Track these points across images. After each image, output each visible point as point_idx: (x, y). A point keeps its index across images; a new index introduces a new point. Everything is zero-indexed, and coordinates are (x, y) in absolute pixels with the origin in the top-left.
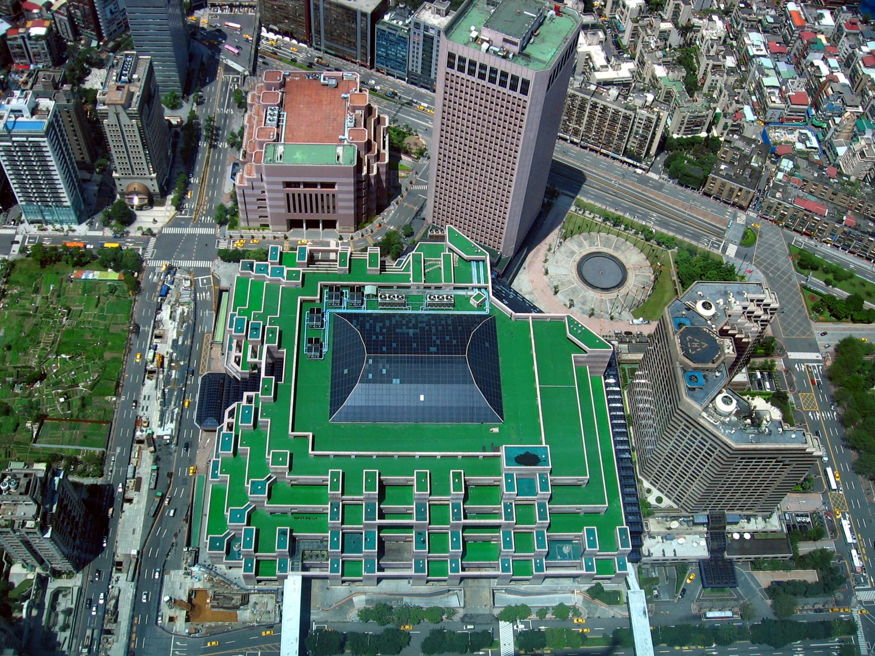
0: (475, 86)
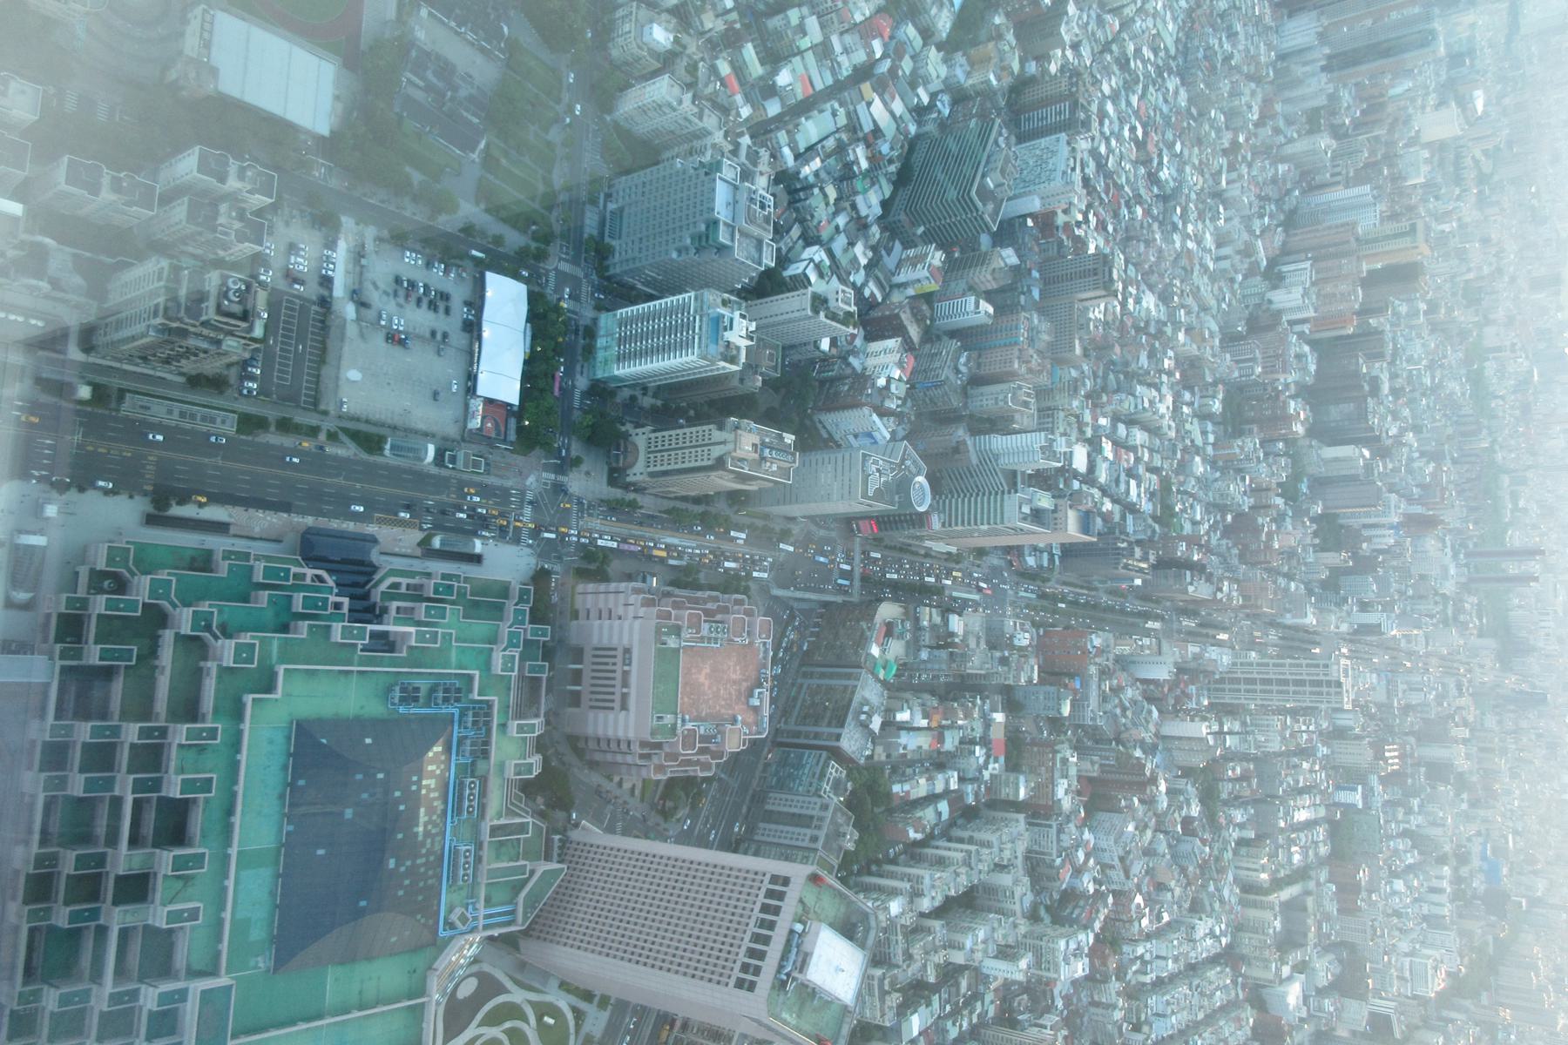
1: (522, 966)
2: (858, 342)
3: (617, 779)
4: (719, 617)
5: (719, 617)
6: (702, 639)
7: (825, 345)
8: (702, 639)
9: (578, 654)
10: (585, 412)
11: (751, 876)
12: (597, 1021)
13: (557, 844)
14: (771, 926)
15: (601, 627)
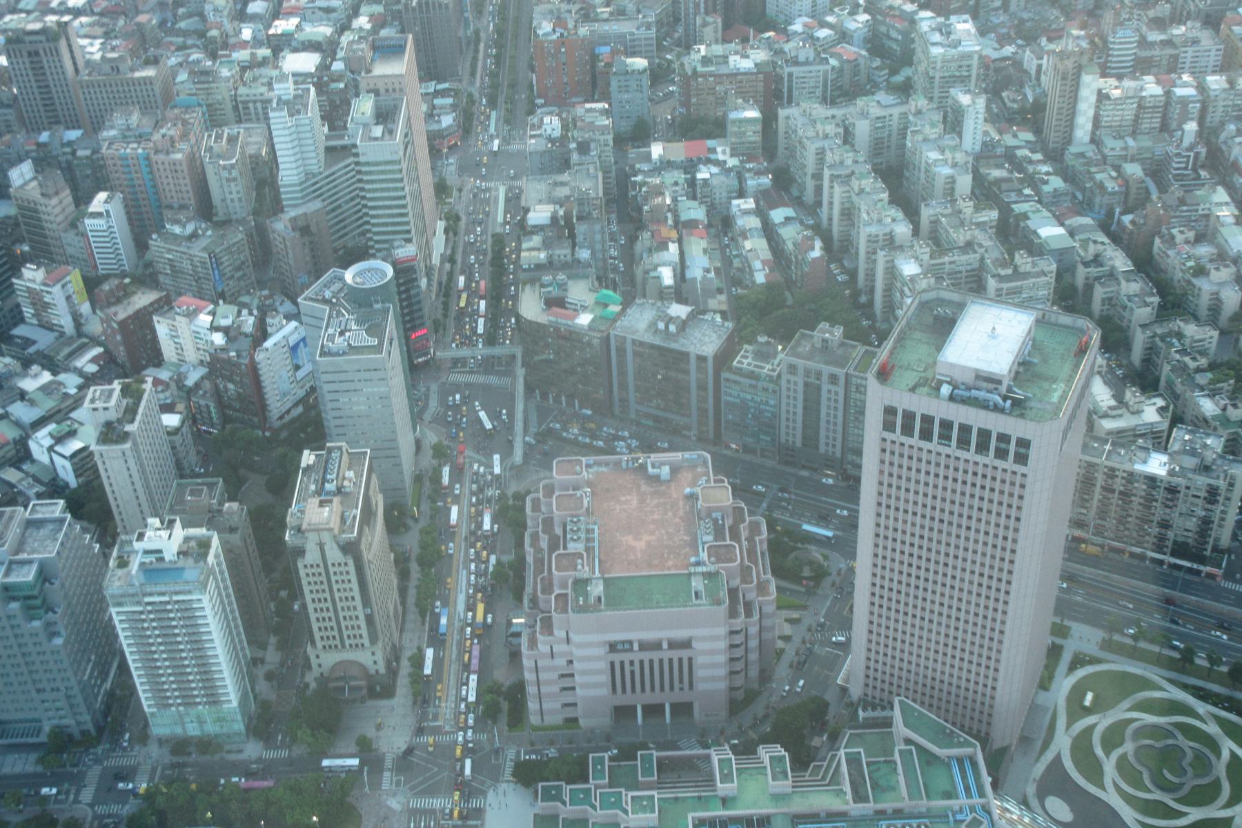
0: (933, 458)
1: (1025, 740)
2: (164, 375)
3: (780, 644)
4: (558, 531)
5: (558, 531)
6: (589, 550)
7: (171, 420)
8: (589, 550)
9: (623, 713)
10: (294, 740)
11: (887, 456)
12: (1084, 637)
13: (870, 714)
14: (946, 425)
15: (585, 686)
